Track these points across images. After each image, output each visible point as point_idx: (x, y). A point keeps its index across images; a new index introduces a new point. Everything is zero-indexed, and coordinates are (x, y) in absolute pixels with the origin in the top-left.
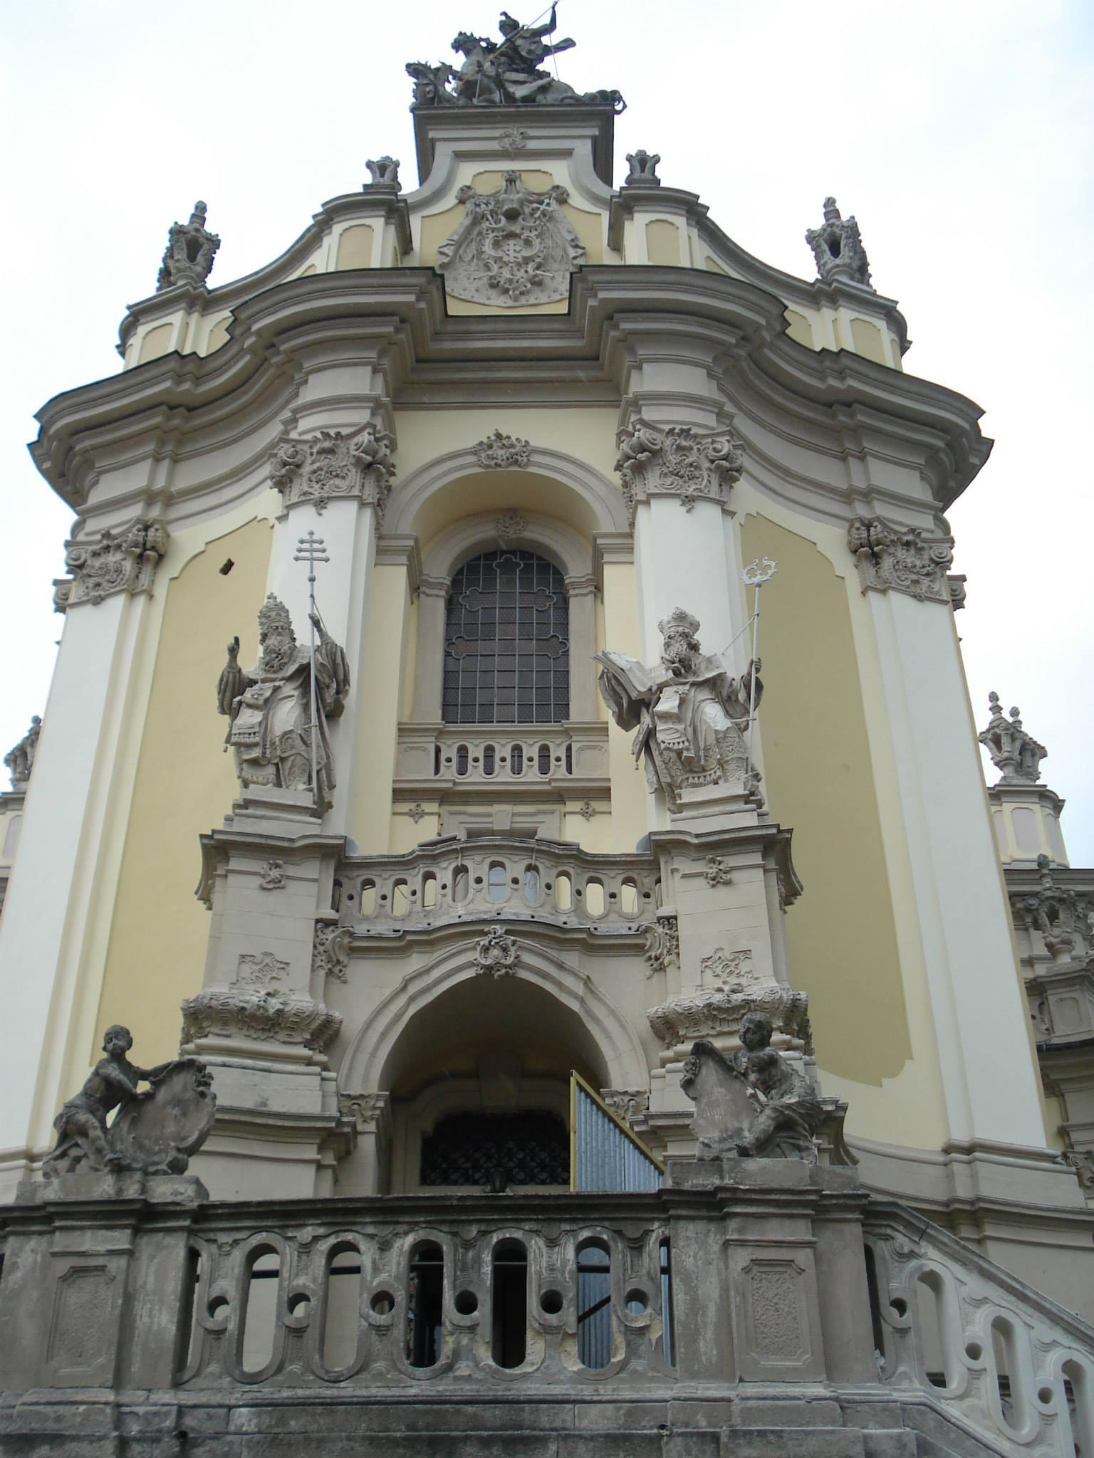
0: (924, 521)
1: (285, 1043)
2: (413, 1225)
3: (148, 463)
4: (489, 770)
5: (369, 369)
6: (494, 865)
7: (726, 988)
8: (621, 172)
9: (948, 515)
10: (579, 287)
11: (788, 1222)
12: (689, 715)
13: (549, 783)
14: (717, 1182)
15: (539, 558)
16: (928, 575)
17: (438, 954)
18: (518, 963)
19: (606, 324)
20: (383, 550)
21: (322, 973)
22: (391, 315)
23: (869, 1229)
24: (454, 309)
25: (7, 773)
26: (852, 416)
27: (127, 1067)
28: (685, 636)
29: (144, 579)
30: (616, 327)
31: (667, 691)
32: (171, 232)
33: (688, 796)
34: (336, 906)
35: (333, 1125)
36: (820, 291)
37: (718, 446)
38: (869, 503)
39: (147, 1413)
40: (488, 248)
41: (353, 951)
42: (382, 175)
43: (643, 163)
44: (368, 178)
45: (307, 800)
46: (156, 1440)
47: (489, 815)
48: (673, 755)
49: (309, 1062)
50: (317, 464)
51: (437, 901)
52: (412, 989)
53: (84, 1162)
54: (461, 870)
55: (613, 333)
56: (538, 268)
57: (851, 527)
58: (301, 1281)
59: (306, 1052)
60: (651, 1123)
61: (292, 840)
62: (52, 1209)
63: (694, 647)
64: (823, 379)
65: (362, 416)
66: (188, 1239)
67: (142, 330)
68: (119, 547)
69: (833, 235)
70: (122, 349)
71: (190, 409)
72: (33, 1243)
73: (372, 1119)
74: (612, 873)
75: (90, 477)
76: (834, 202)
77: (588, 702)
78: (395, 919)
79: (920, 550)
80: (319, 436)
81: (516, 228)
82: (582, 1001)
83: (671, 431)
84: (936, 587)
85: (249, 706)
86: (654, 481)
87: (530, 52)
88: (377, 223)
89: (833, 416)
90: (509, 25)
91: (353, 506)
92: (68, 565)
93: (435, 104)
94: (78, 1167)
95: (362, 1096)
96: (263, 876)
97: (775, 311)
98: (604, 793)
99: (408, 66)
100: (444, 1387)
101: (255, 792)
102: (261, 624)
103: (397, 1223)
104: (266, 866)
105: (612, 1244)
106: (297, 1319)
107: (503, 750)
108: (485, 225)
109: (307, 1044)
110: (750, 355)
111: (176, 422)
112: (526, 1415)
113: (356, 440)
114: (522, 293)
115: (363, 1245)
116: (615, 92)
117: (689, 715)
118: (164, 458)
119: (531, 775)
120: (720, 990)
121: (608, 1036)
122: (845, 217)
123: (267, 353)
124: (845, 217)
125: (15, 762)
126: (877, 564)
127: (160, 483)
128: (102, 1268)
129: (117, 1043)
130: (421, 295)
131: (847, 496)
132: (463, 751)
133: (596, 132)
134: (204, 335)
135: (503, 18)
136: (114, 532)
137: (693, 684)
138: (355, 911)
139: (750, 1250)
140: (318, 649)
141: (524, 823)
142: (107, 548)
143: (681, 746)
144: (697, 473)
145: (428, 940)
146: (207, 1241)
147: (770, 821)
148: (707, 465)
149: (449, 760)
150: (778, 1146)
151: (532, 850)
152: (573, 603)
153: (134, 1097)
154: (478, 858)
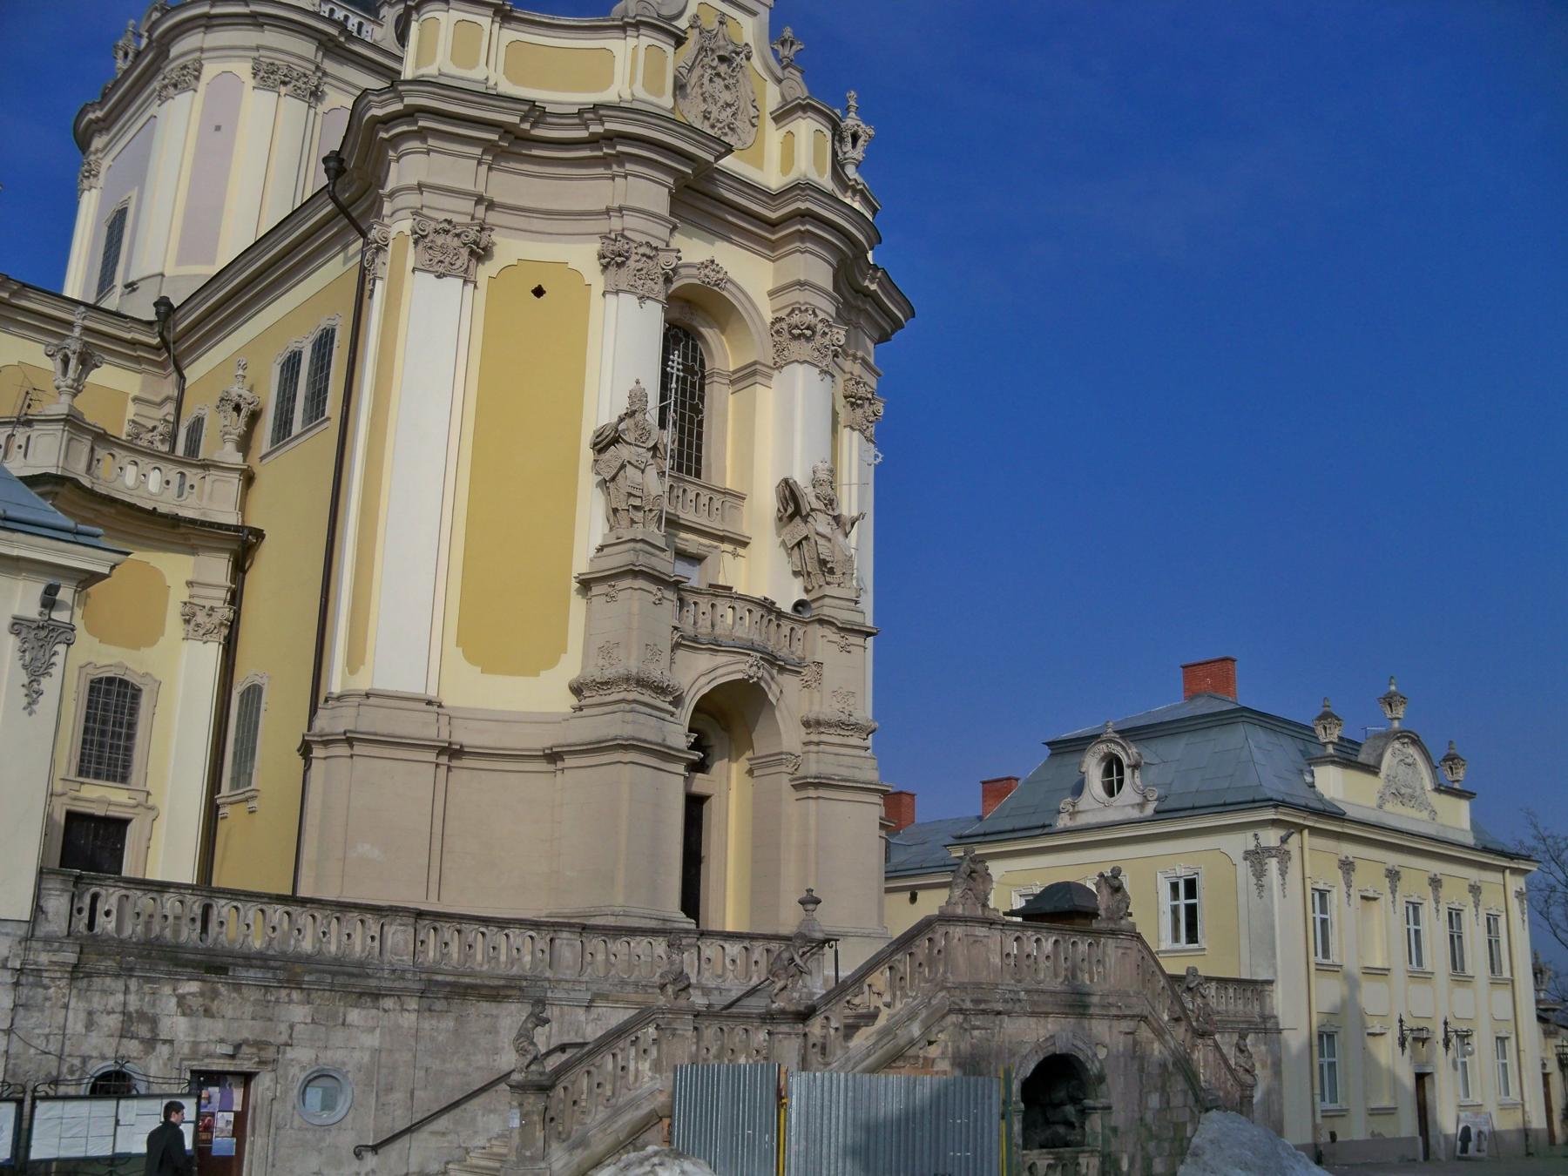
17: (722, 659)
33: (828, 590)
40: (706, 80)
50: (640, 265)
59: (671, 708)
68: (458, 235)
81: (723, 68)
88: (670, 50)
136: (456, 219)
142: (447, 232)
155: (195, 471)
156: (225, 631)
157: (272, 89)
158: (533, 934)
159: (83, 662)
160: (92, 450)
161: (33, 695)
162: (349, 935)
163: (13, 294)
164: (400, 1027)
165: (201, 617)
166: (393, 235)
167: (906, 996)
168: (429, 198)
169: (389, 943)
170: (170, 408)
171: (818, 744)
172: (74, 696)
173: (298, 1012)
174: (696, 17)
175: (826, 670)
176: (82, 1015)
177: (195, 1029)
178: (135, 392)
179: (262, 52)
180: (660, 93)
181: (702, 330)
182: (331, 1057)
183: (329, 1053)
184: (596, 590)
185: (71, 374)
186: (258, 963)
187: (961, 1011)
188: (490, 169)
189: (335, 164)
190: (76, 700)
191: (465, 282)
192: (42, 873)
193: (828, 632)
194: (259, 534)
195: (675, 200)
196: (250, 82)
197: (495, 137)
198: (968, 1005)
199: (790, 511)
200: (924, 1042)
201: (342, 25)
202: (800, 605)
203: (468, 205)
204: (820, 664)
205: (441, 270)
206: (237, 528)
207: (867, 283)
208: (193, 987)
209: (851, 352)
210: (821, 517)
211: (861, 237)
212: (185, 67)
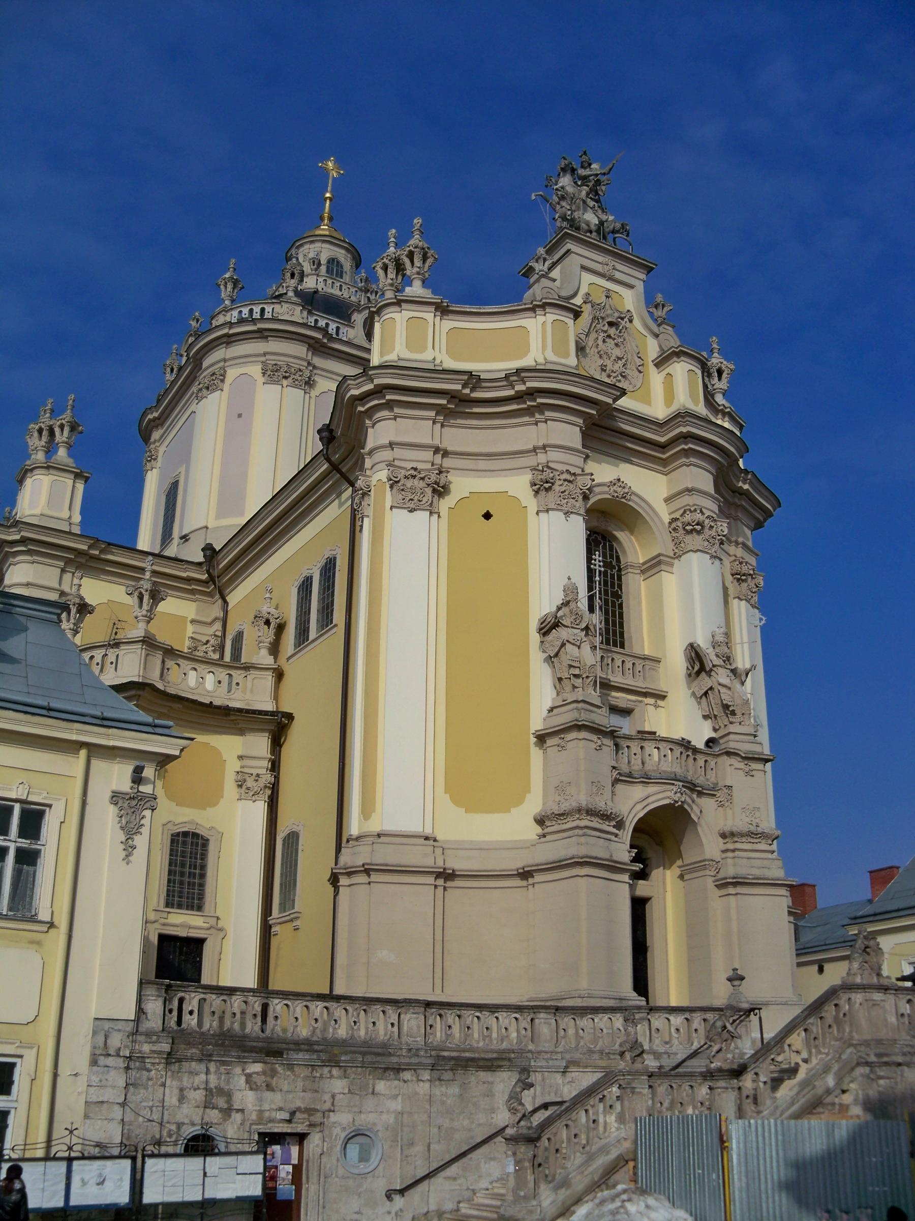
17: (652, 789)
22: (596, 404)
33: (732, 728)
40: (600, 342)
50: (563, 488)
59: (615, 830)
67: (406, 314)
68: (423, 479)
71: (460, 401)
81: (612, 331)
88: (570, 322)
109: (614, 827)
136: (420, 466)
141: (630, 705)
142: (414, 477)
155: (239, 672)
156: (269, 792)
157: (277, 383)
158: (517, 1016)
159: (165, 821)
160: (163, 662)
161: (129, 849)
162: (374, 1023)
163: (102, 551)
164: (417, 1094)
165: (250, 783)
166: (374, 482)
167: (820, 1053)
168: (398, 452)
169: (405, 1028)
170: (218, 626)
171: (733, 851)
172: (160, 846)
173: (338, 1085)
174: (588, 294)
176: (176, 1092)
177: (260, 1100)
178: (192, 616)
179: (268, 357)
180: (566, 355)
181: (615, 533)
182: (365, 1119)
183: (363, 1116)
184: (550, 742)
185: (145, 606)
186: (306, 1047)
187: (867, 1064)
188: (442, 426)
189: (327, 434)
190: (162, 850)
191: (431, 513)
192: (141, 984)
193: (734, 761)
194: (290, 717)
195: (586, 435)
196: (261, 379)
197: (444, 402)
198: (873, 1058)
199: (696, 668)
200: (838, 1091)
201: (325, 331)
202: (710, 742)
203: (428, 455)
205: (412, 506)
206: (273, 713)
207: (740, 484)
208: (257, 1067)
209: (733, 539)
210: (721, 671)
211: (732, 449)
212: (214, 374)
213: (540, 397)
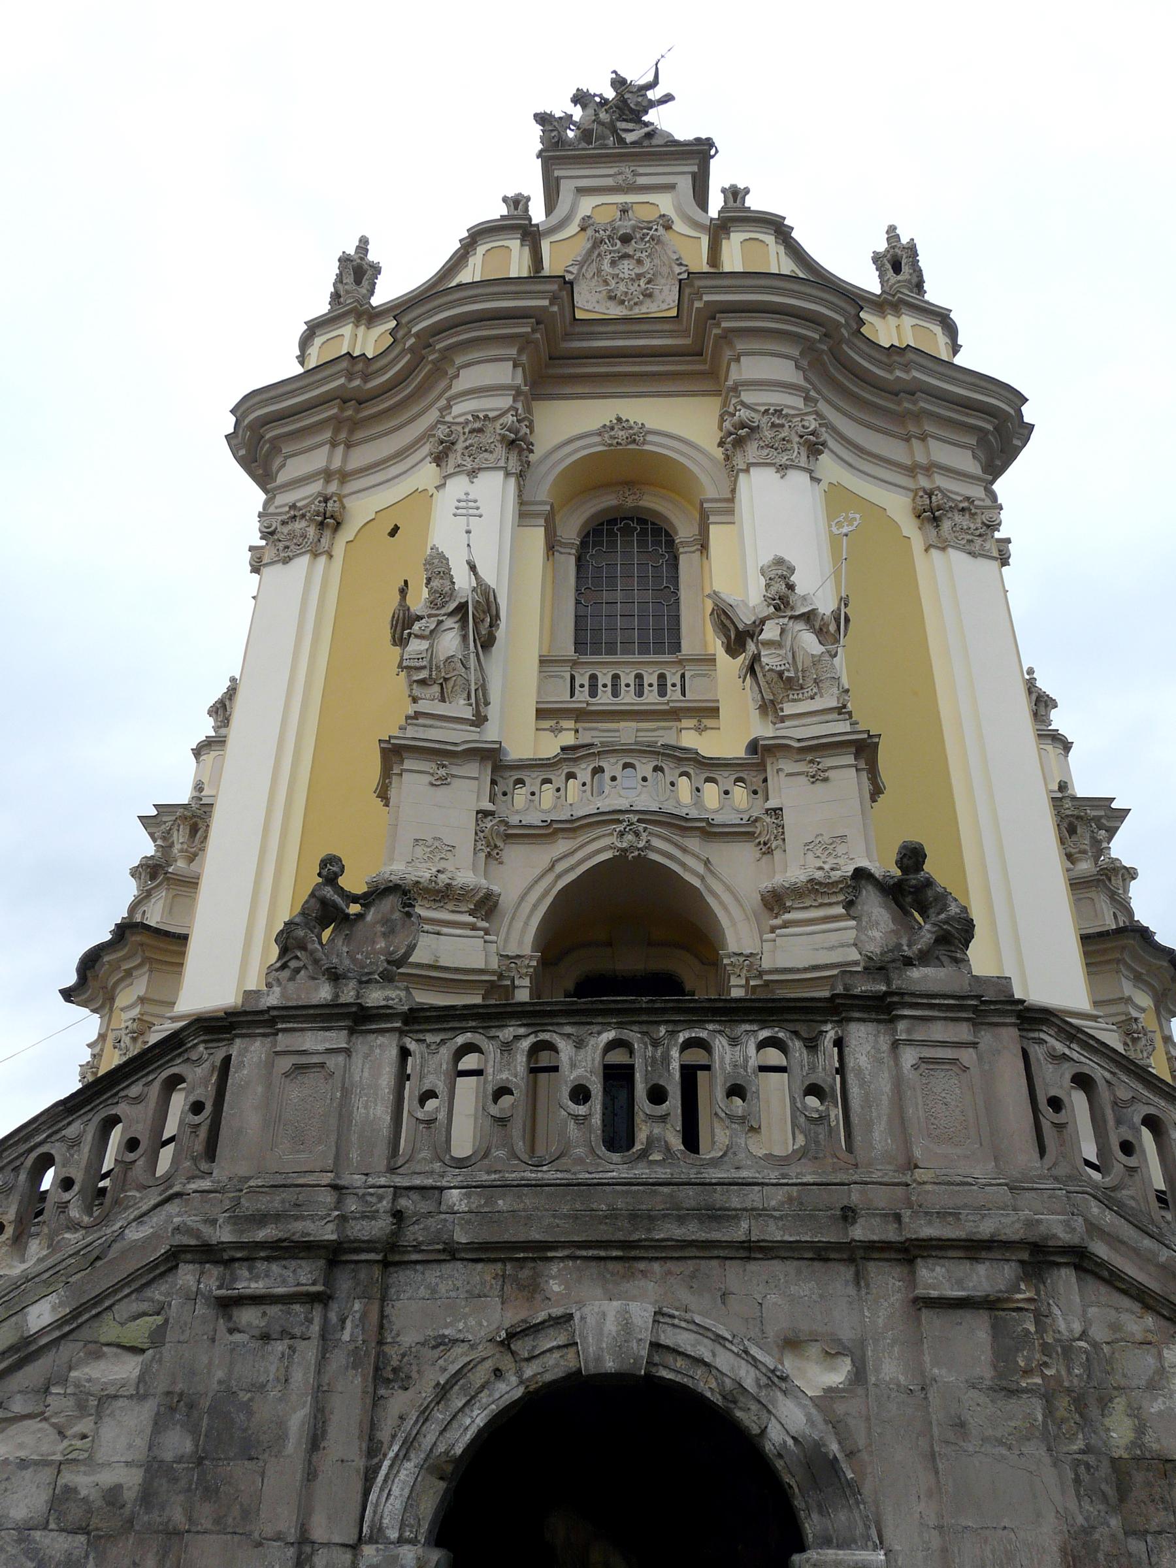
0: (977, 492)
1: (453, 912)
2: (606, 1026)
3: (328, 446)
4: (615, 694)
5: (511, 363)
6: (626, 766)
7: (827, 867)
8: (716, 203)
9: (995, 487)
10: (687, 291)
11: (951, 1025)
12: (789, 643)
13: (667, 703)
14: (884, 988)
15: (653, 523)
16: (980, 535)
18: (649, 847)
19: (710, 322)
20: (524, 514)
21: (483, 855)
23: (1024, 1034)
24: (579, 315)
25: (211, 722)
26: (915, 403)
27: (341, 891)
28: (783, 577)
29: (325, 542)
30: (718, 325)
31: (769, 625)
32: (339, 260)
34: (492, 800)
35: (495, 978)
36: (886, 300)
37: (806, 424)
38: (929, 476)
39: (364, 1195)
40: (606, 266)
41: (508, 836)
42: (516, 208)
43: (735, 194)
44: (503, 210)
45: (468, 713)
46: (373, 1218)
47: (618, 731)
48: (775, 676)
49: (474, 928)
50: (467, 444)
51: (576, 797)
52: (560, 868)
53: (302, 972)
54: (598, 770)
55: (716, 331)
56: (648, 282)
57: (916, 495)
58: (504, 1076)
59: (471, 919)
60: (766, 977)
61: (456, 744)
62: (275, 1013)
63: (791, 587)
64: (891, 372)
65: (505, 402)
66: (400, 1039)
67: (318, 341)
69: (895, 256)
70: (302, 359)
72: (258, 1043)
73: (526, 975)
74: (726, 774)
75: (277, 462)
76: (895, 228)
77: (700, 634)
78: (544, 812)
79: (973, 515)
80: (471, 418)
82: (702, 879)
83: (767, 411)
84: (987, 546)
85: (417, 636)
86: (752, 451)
87: (638, 104)
88: (515, 244)
89: (899, 404)
90: (619, 83)
91: (501, 474)
92: (261, 532)
93: (561, 147)
94: (298, 976)
95: (518, 957)
96: (432, 775)
97: (853, 311)
98: (714, 712)
99: (536, 115)
100: (641, 1171)
101: (424, 706)
102: (426, 570)
103: (592, 1023)
104: (434, 766)
105: (790, 1043)
106: (501, 1110)
107: (627, 677)
108: (604, 247)
110: (830, 350)
111: (349, 413)
112: (717, 1196)
113: (501, 421)
114: (636, 304)
115: (562, 1044)
116: (708, 139)
117: (789, 643)
118: (339, 444)
119: (651, 697)
120: (821, 868)
121: (725, 908)
122: (904, 240)
123: (423, 352)
124: (904, 240)
125: (217, 713)
126: (938, 526)
127: (336, 464)
128: (322, 1065)
129: (331, 870)
130: (554, 300)
131: (911, 470)
132: (593, 678)
133: (695, 169)
134: (369, 341)
135: (614, 76)
137: (791, 618)
138: (510, 806)
139: (918, 1049)
140: (474, 589)
141: (645, 737)
143: (783, 668)
144: (789, 446)
145: (573, 827)
146: (417, 1041)
147: (860, 728)
148: (798, 439)
149: (582, 686)
150: (938, 958)
151: (658, 753)
152: (683, 559)
153: (347, 916)
154: (613, 760)
171: (785, 925)
175: (788, 818)
187: (207, 1253)
197: (335, 411)
198: (224, 1235)
202: (754, 747)
204: (777, 812)
213: (439, 341)
